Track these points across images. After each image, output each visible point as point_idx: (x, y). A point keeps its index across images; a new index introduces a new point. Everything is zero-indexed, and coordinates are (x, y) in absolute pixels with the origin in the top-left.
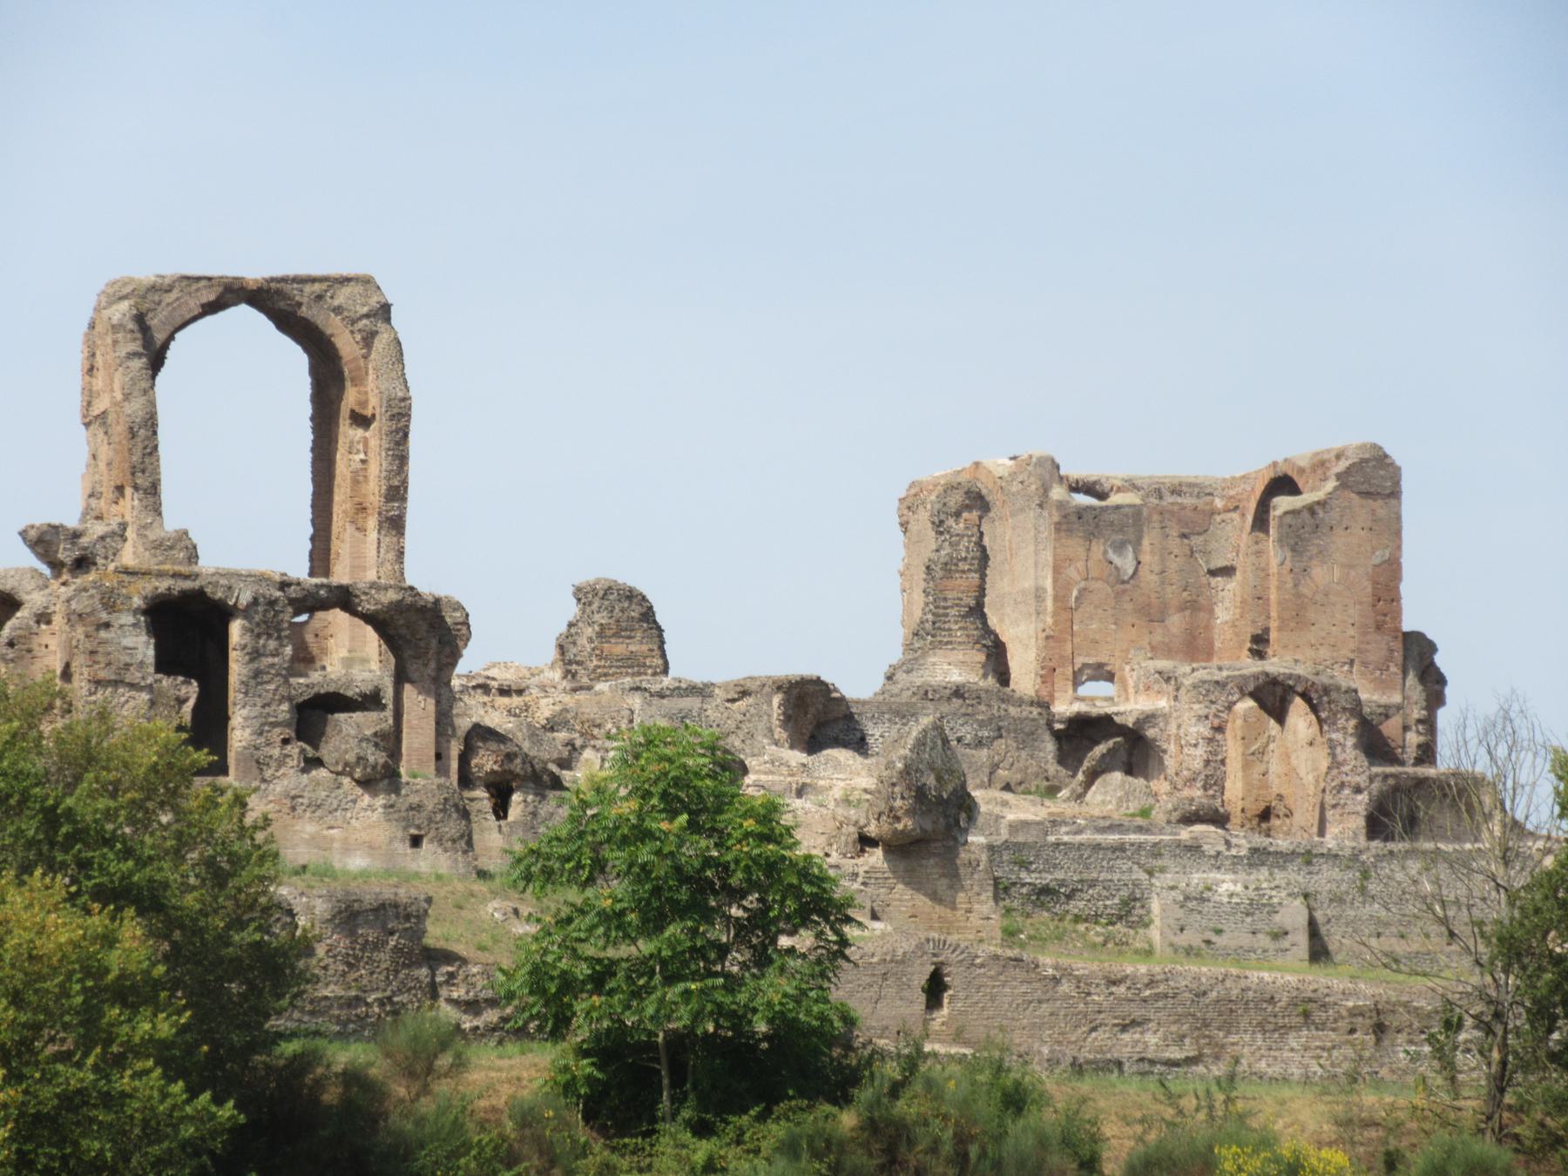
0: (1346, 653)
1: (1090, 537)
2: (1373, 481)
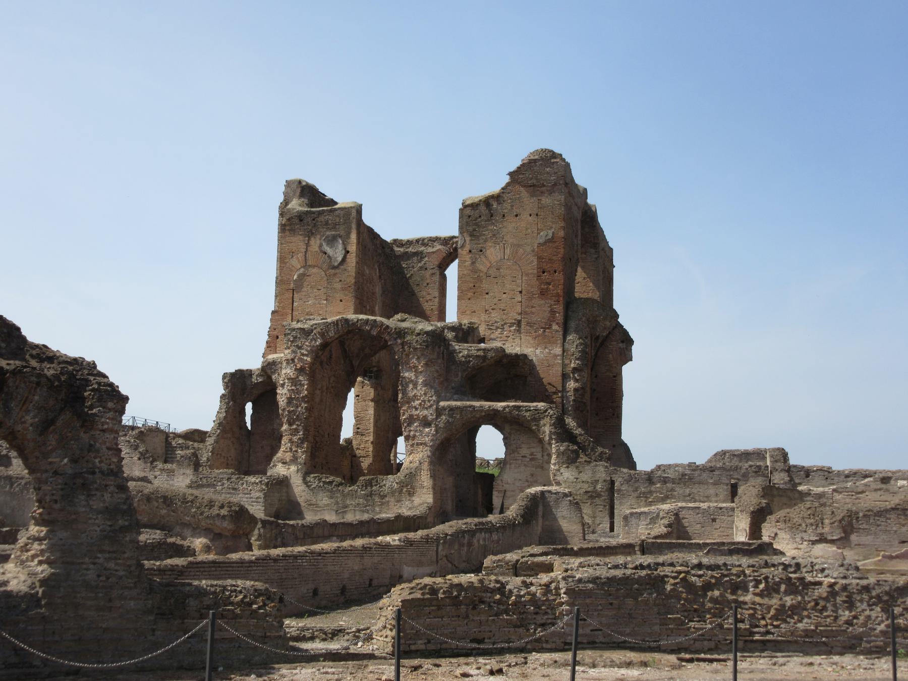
0: (514, 315)
1: (310, 234)
2: (539, 177)
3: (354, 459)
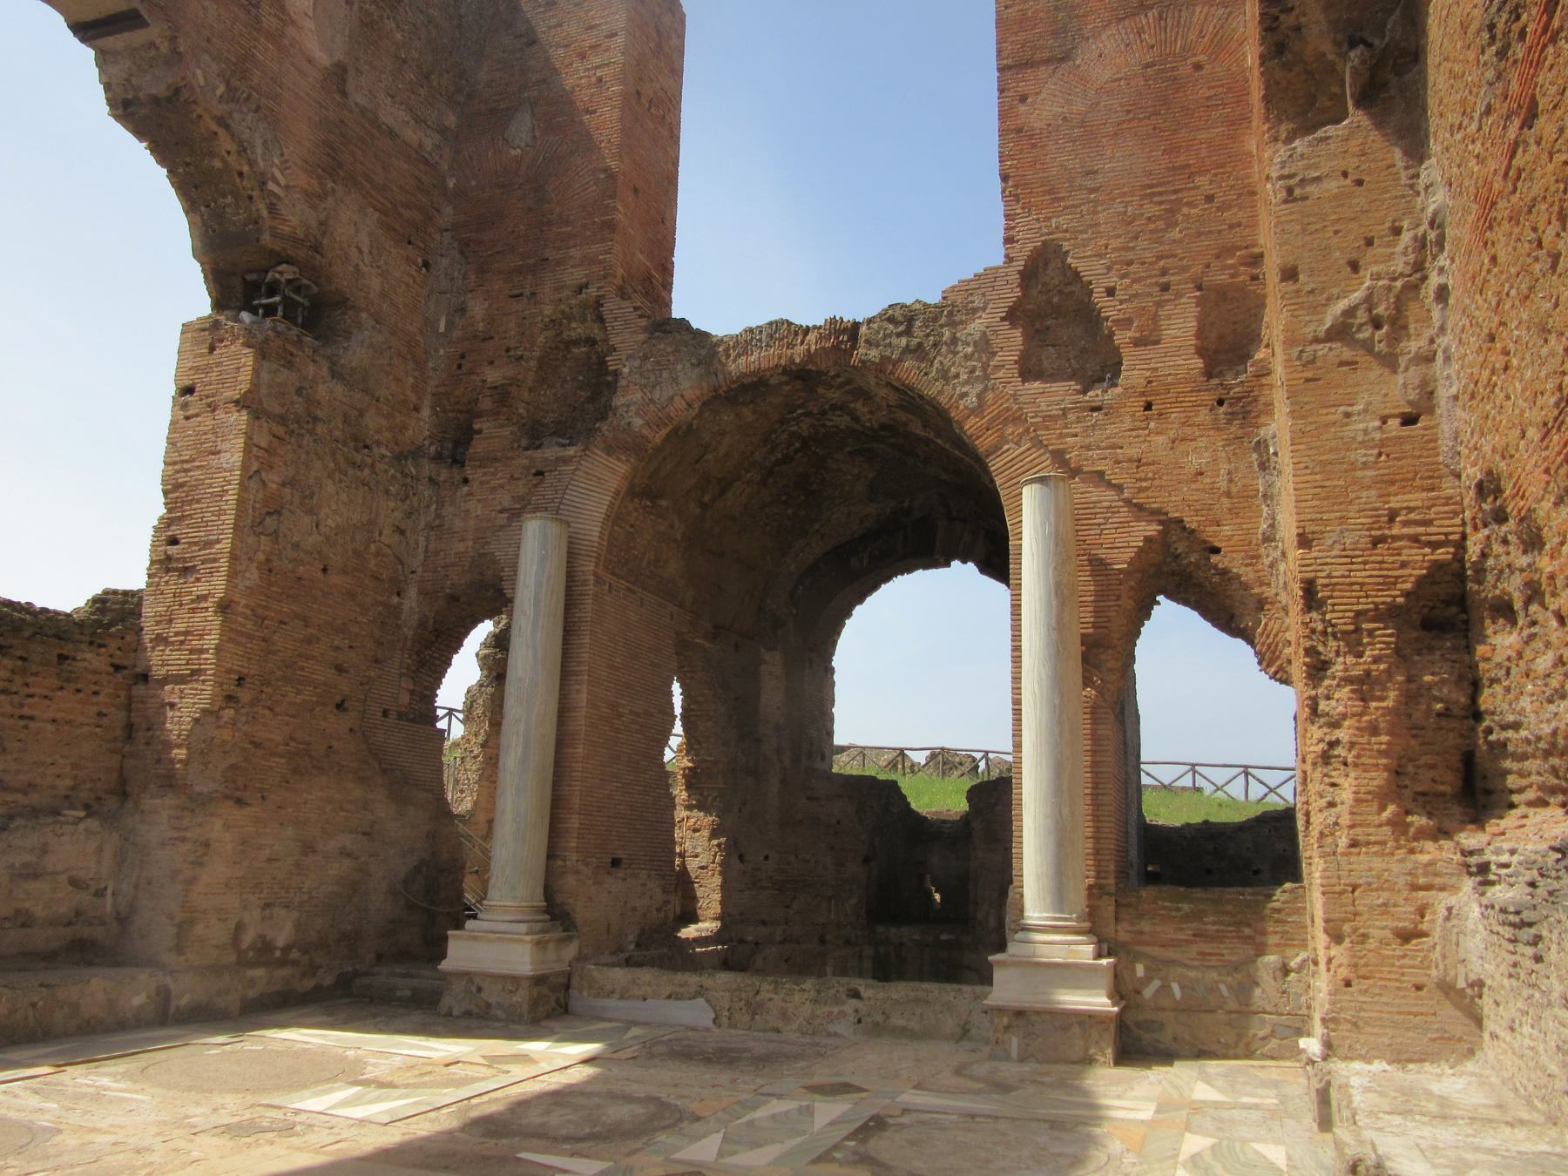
3: (140, 690)
